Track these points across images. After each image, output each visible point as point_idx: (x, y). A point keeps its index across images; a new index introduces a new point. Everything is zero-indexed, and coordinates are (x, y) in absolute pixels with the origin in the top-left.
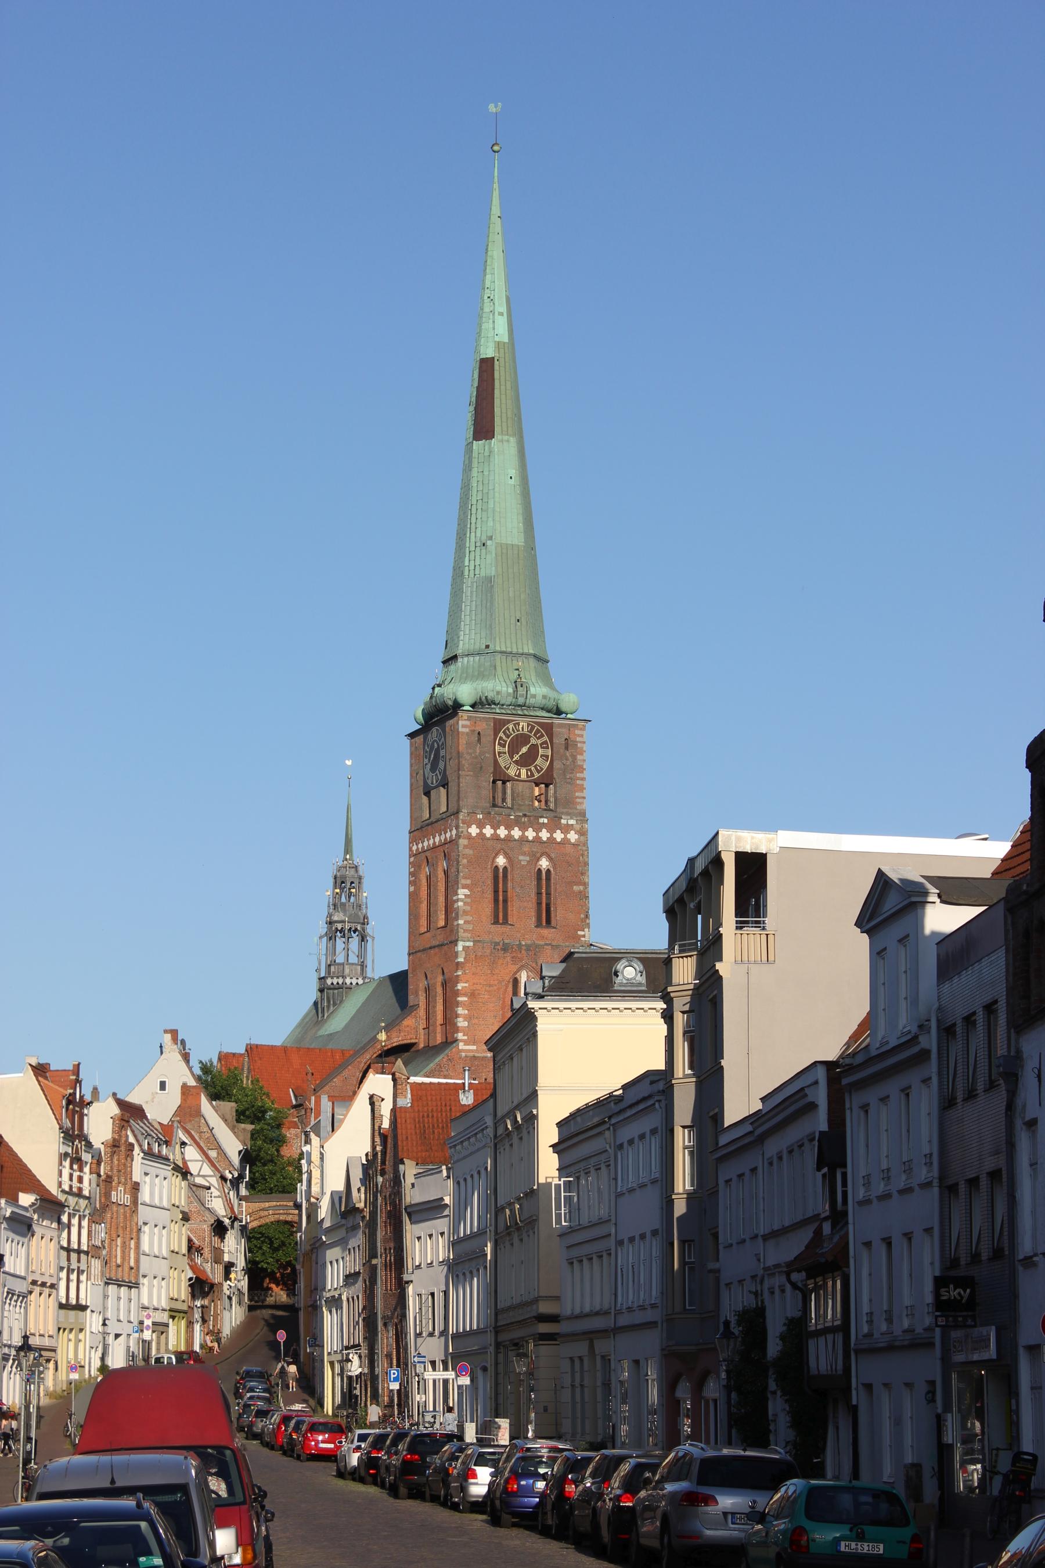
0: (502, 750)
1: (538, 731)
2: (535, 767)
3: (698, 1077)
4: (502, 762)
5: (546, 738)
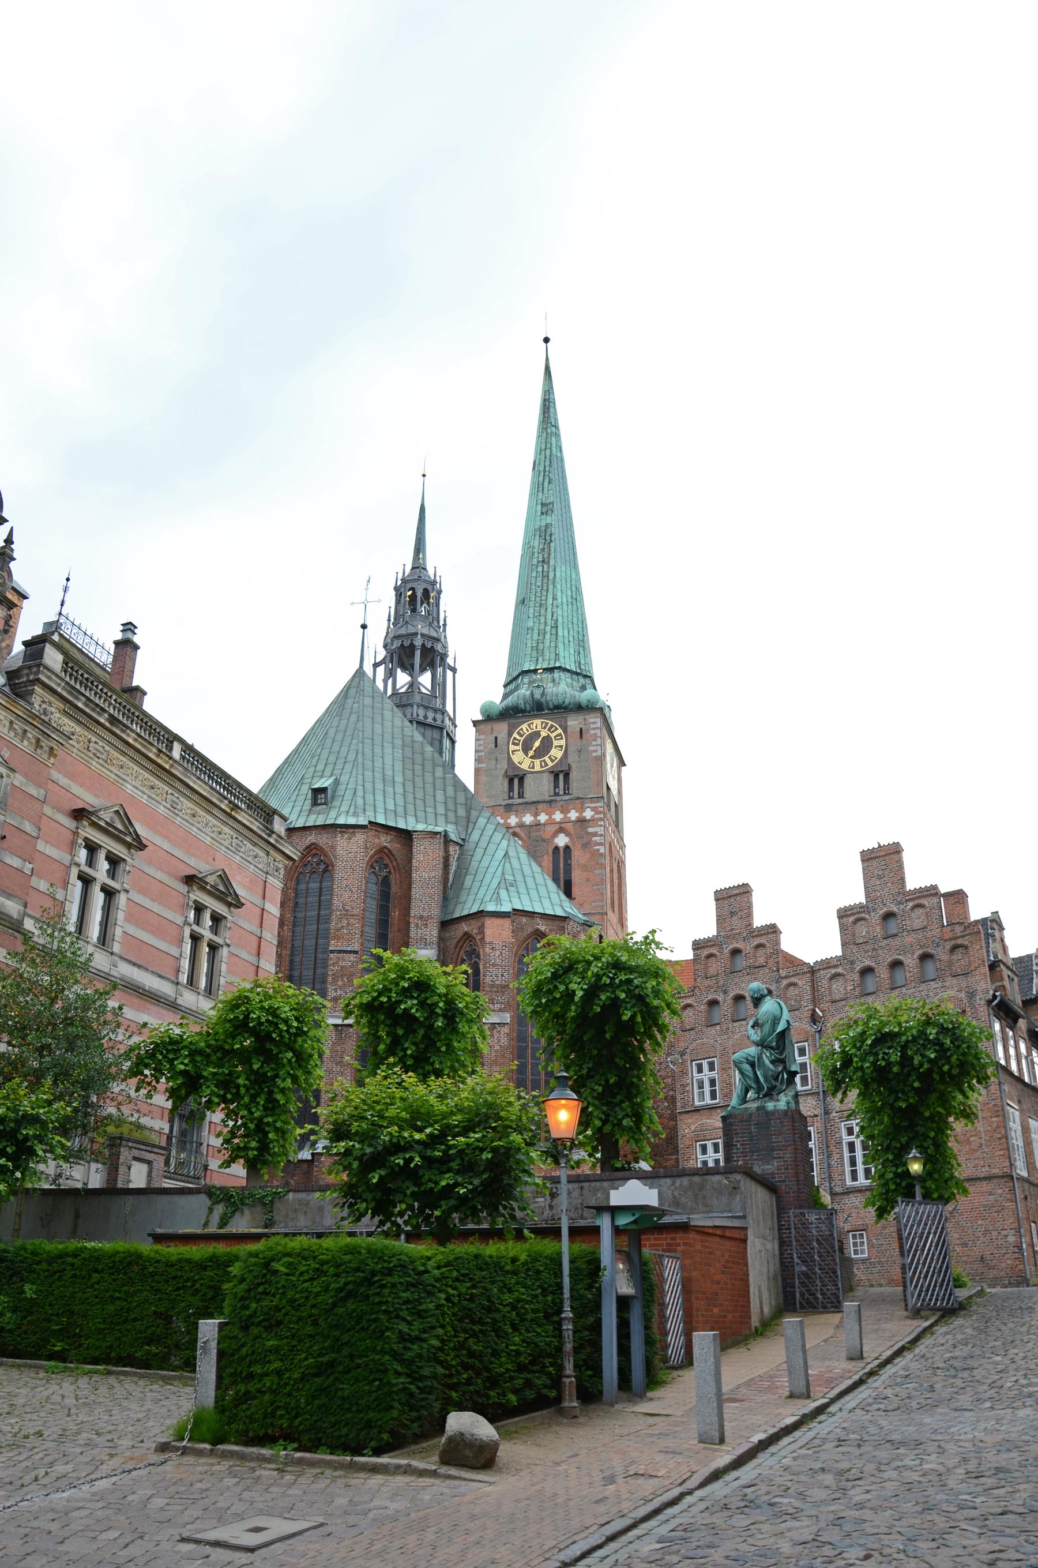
0: (516, 748)
2: (550, 758)
3: (944, 1100)
5: (560, 731)
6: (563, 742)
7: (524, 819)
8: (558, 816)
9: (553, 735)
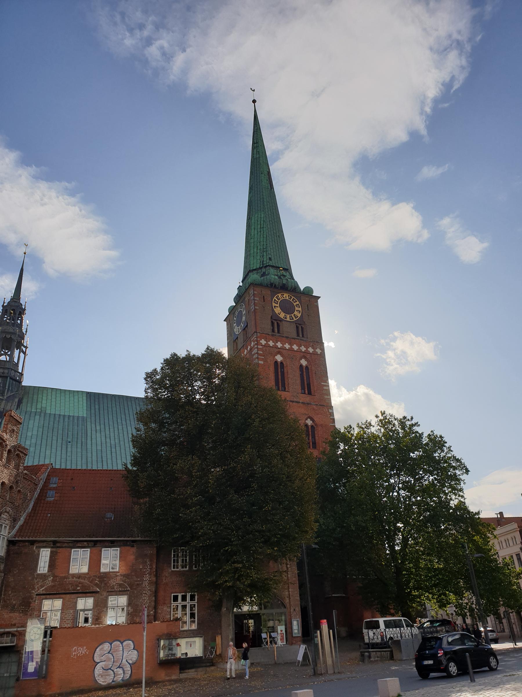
1: (293, 299)
2: (294, 315)
4: (278, 310)
5: (298, 303)
6: (300, 309)
7: (285, 346)
8: (303, 349)
9: (295, 304)
